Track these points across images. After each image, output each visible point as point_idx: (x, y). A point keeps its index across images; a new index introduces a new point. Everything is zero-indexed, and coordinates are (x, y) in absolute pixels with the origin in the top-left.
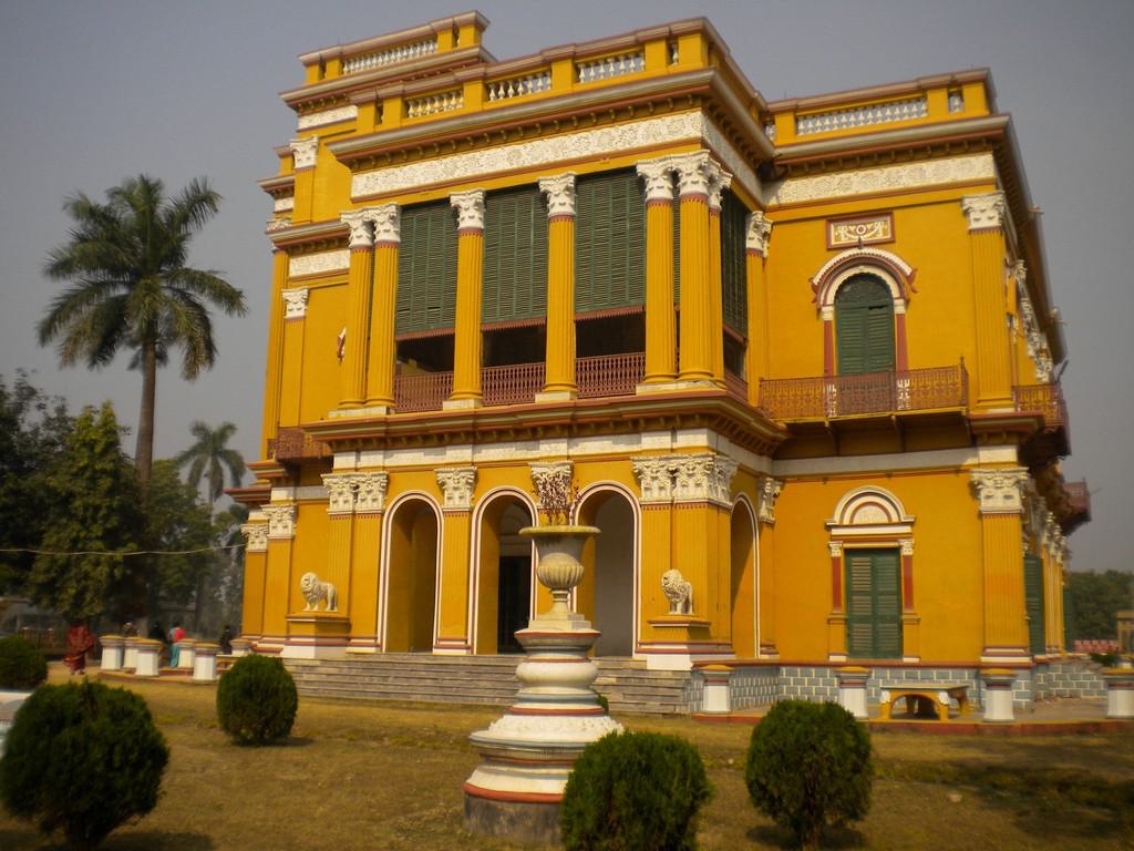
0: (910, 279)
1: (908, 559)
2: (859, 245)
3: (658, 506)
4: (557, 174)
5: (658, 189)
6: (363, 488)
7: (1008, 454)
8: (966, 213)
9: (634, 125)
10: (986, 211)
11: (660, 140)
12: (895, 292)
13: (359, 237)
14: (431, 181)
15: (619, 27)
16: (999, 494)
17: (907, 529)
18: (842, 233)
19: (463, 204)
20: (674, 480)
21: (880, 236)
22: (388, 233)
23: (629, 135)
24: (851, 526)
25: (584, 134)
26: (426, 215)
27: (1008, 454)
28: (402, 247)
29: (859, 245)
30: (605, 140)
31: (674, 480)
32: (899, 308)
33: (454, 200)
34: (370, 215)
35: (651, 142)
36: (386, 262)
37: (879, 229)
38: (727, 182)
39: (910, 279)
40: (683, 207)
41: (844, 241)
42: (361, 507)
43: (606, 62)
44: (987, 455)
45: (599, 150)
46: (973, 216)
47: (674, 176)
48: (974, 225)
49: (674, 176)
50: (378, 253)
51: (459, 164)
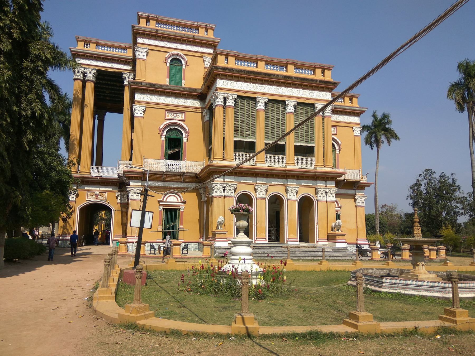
3: (323, 201)
4: (292, 100)
6: (227, 188)
8: (353, 131)
9: (313, 91)
11: (320, 98)
14: (248, 90)
15: (311, 62)
19: (260, 101)
20: (326, 195)
22: (230, 103)
23: (311, 94)
25: (298, 90)
30: (305, 93)
31: (326, 195)
32: (337, 152)
33: (258, 99)
35: (318, 98)
36: (230, 113)
40: (326, 120)
42: (227, 194)
43: (302, 69)
45: (303, 96)
46: (355, 132)
48: (355, 134)
51: (258, 87)
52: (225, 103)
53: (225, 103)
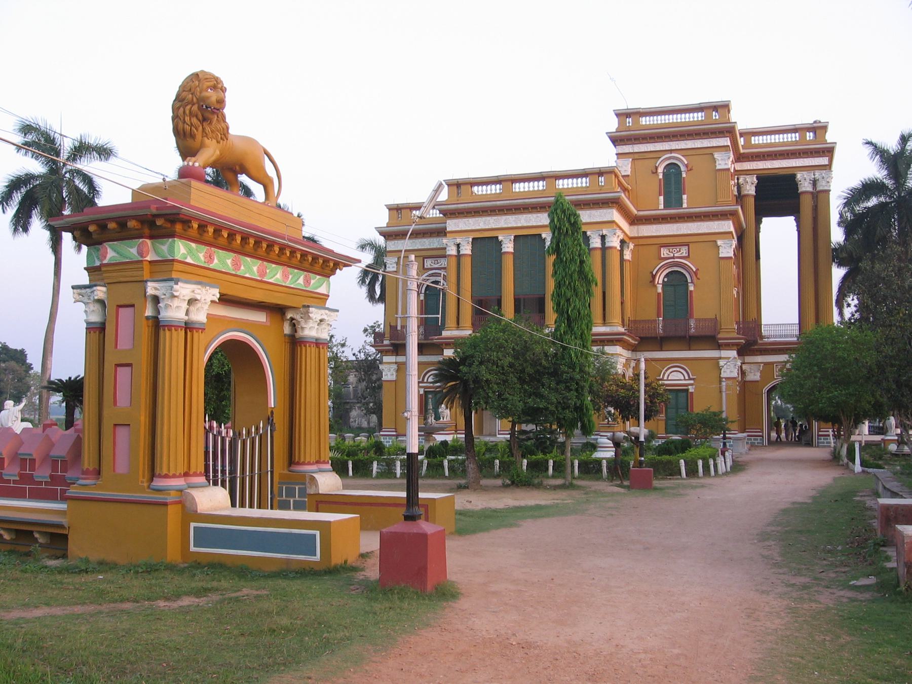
0: (696, 273)
1: (692, 393)
2: (673, 258)
5: (596, 243)
7: (733, 353)
10: (727, 249)
12: (689, 280)
13: (452, 251)
16: (728, 371)
17: (692, 382)
18: (664, 252)
21: (684, 255)
22: (467, 249)
24: (668, 380)
26: (486, 245)
27: (733, 353)
28: (473, 256)
29: (673, 258)
32: (691, 288)
34: (458, 241)
37: (684, 251)
38: (622, 237)
39: (696, 273)
41: (666, 256)
44: (725, 353)
47: (603, 238)
49: (603, 238)
50: (462, 260)
52: (459, 251)
53: (459, 251)
